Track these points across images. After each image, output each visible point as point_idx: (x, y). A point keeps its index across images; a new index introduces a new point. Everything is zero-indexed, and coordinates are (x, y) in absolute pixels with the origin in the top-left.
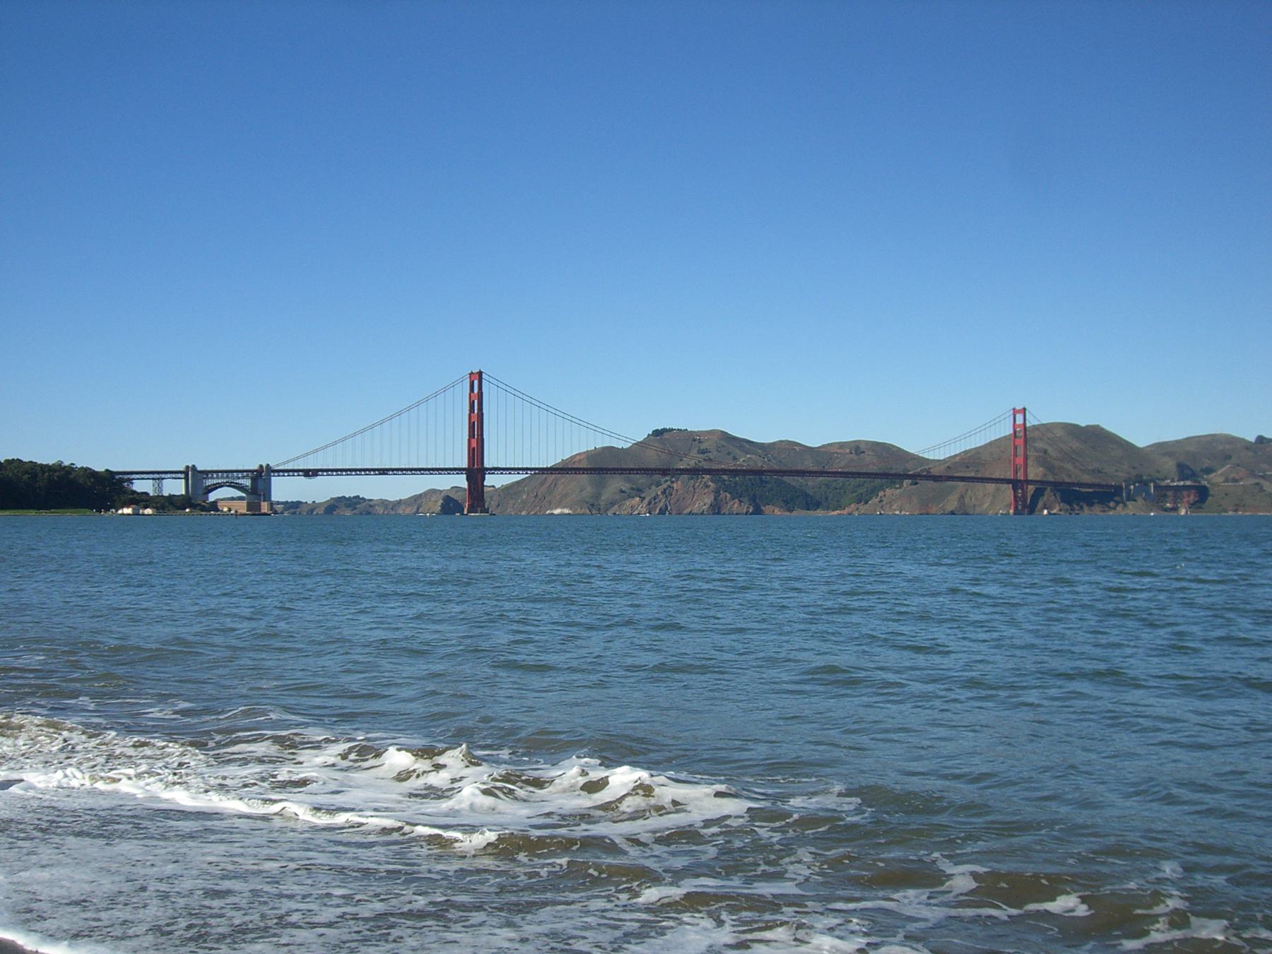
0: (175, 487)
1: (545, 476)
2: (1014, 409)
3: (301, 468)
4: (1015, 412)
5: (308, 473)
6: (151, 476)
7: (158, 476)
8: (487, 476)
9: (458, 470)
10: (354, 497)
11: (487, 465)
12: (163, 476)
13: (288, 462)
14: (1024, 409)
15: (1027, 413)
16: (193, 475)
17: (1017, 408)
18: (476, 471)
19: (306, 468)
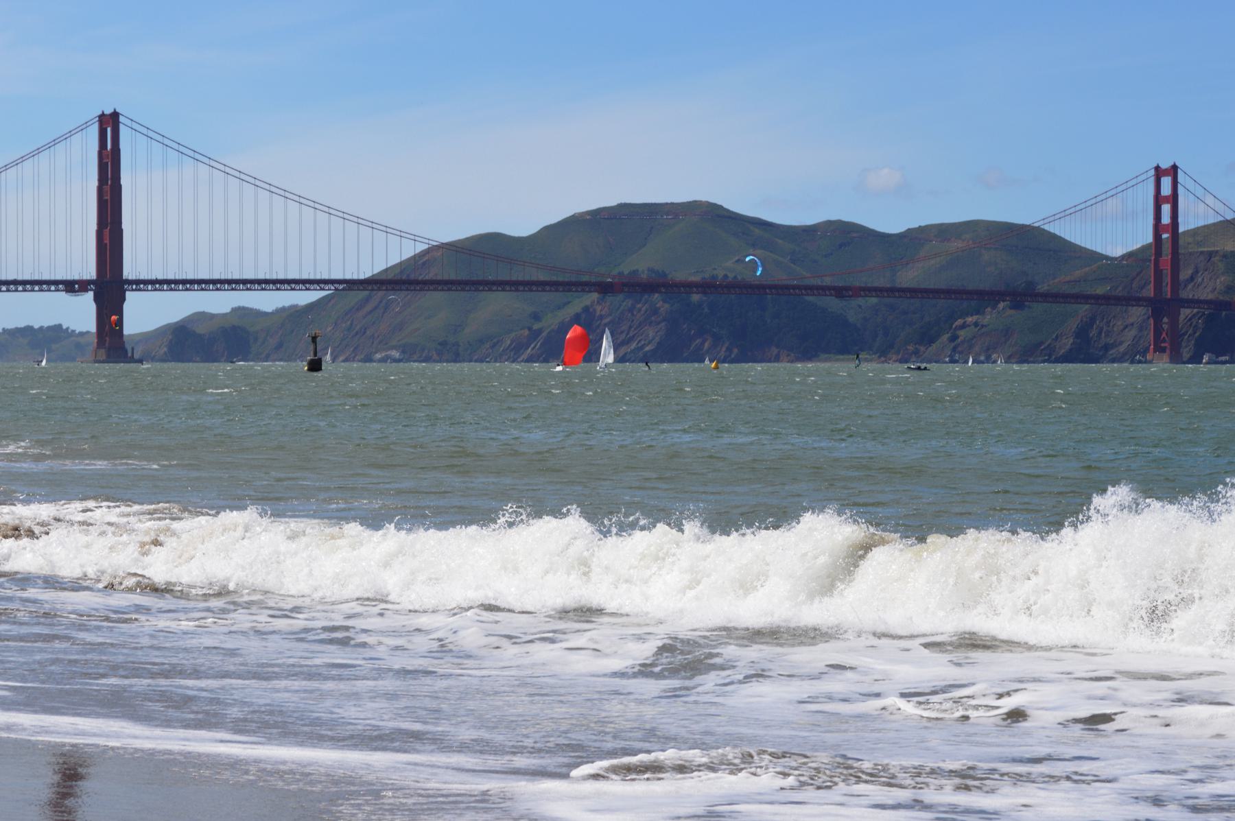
1: (366, 293)
2: (1157, 168)
3: (59, 277)
4: (1159, 173)
8: (128, 294)
9: (72, 286)
10: (50, 328)
14: (1175, 168)
15: (1180, 174)
17: (1165, 165)
19: (69, 278)
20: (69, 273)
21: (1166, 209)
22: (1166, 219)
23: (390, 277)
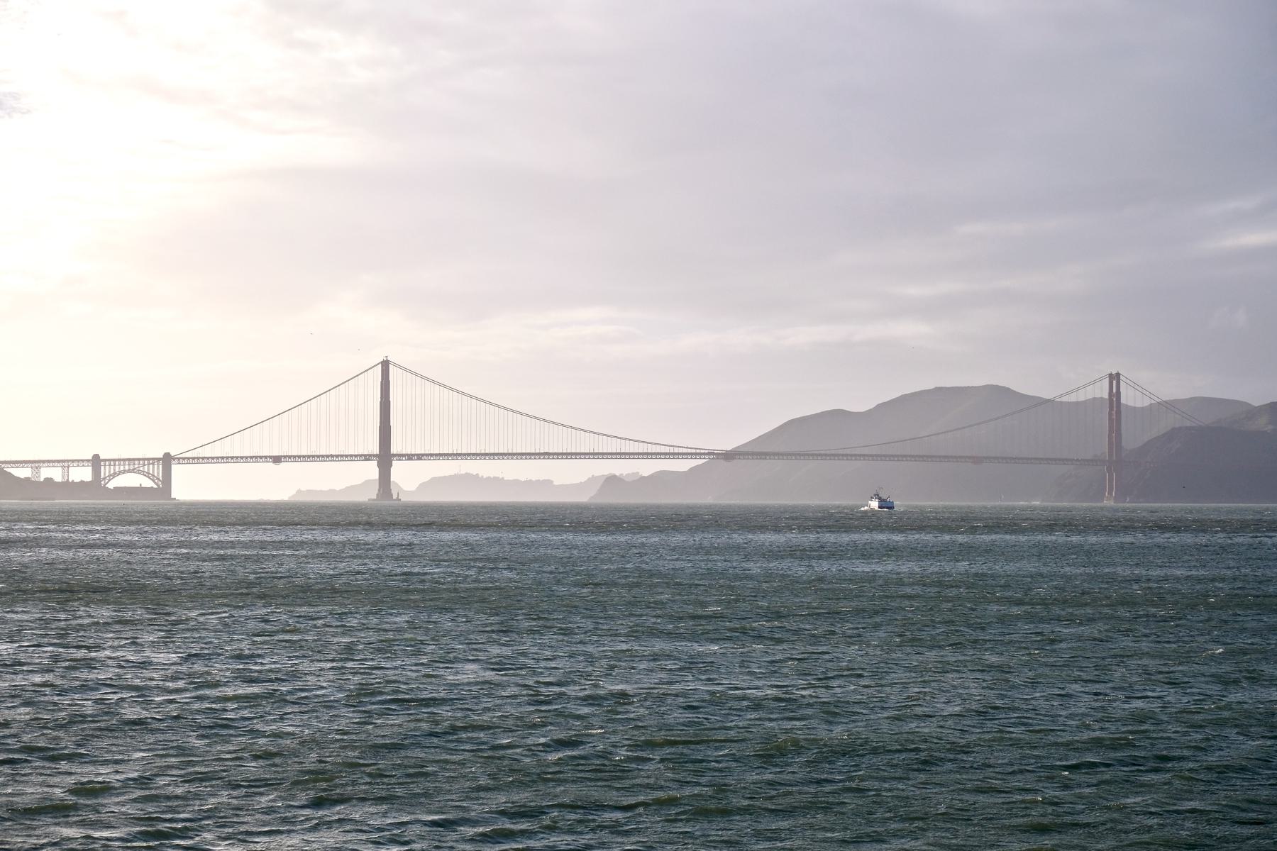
0: (82, 474)
7: (65, 463)
8: (394, 463)
16: (96, 461)
18: (385, 458)
20: (356, 451)
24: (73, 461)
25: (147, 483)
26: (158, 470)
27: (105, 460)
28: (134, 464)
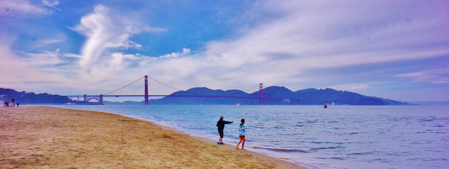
0: (82, 99)
3: (116, 95)
5: (117, 96)
6: (77, 97)
7: (78, 96)
8: (149, 97)
11: (149, 95)
12: (79, 97)
13: (106, 94)
14: (262, 84)
16: (85, 96)
17: (261, 83)
18: (146, 96)
21: (261, 88)
22: (261, 89)
23: (172, 95)
24: (80, 96)
25: (97, 101)
26: (99, 98)
27: (88, 96)
28: (94, 97)
